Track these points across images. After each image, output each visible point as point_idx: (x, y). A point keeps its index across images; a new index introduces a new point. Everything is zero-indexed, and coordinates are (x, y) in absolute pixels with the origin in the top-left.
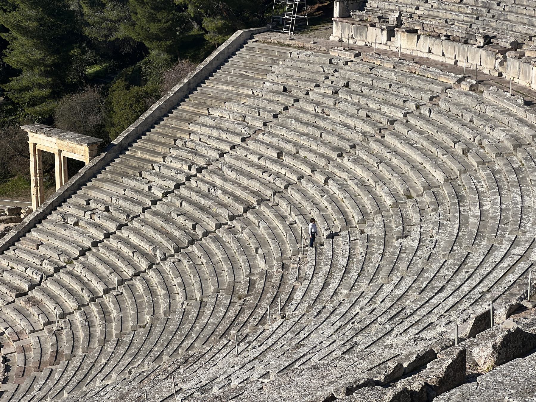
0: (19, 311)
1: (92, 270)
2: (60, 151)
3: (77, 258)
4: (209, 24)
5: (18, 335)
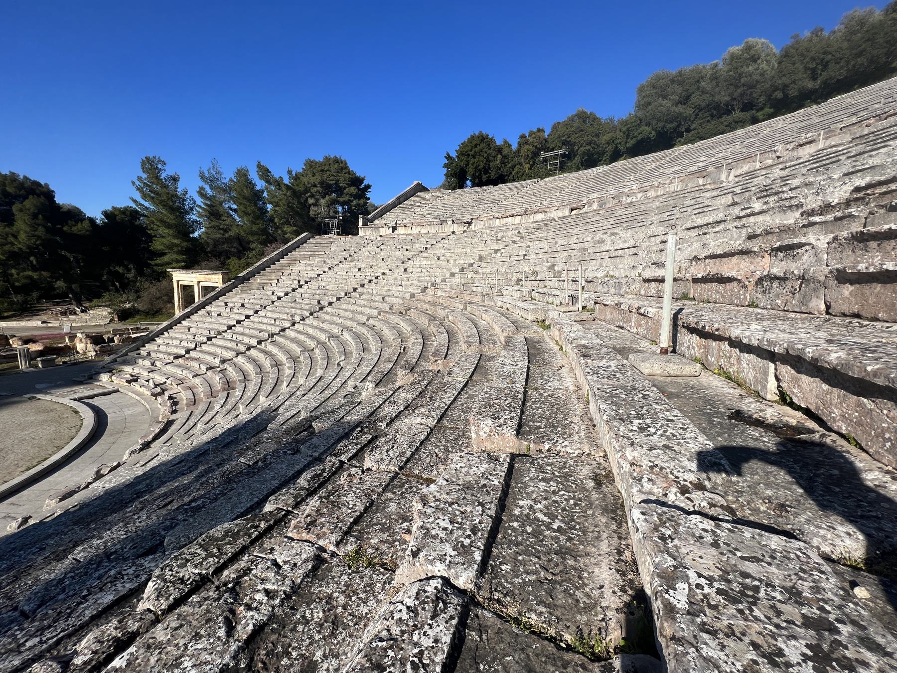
0: (179, 366)
1: (243, 334)
2: (199, 282)
3: (225, 332)
4: (287, 229)
5: (181, 382)
